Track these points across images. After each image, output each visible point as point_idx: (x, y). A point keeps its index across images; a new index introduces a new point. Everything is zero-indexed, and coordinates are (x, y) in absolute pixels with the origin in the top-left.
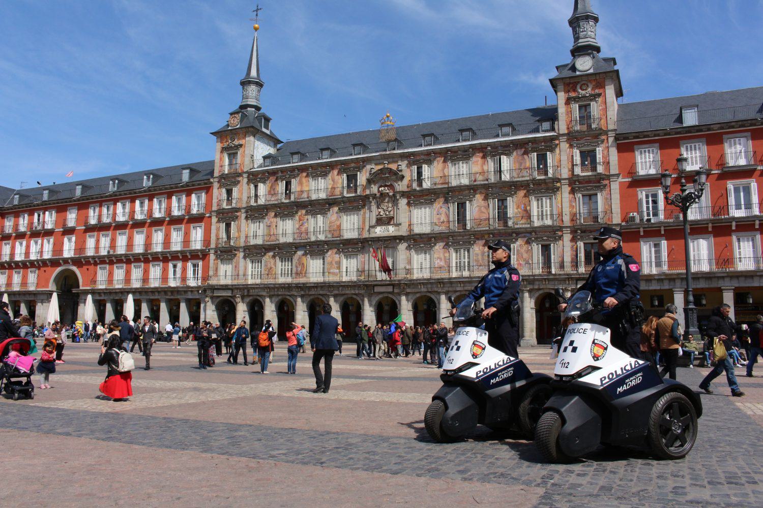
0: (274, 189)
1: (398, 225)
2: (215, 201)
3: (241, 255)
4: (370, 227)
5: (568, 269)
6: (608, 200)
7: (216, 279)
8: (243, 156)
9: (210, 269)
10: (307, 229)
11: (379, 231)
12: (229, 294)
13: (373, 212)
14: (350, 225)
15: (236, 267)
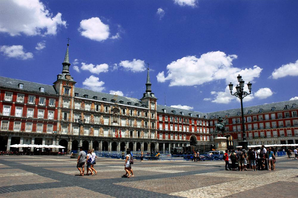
0: (83, 106)
1: (118, 123)
2: (60, 104)
3: (71, 125)
4: (112, 123)
5: (149, 138)
6: (155, 124)
7: (60, 132)
8: (72, 91)
9: (58, 128)
10: (94, 120)
11: (114, 124)
12: (67, 138)
13: (112, 119)
14: (106, 122)
15: (69, 129)
